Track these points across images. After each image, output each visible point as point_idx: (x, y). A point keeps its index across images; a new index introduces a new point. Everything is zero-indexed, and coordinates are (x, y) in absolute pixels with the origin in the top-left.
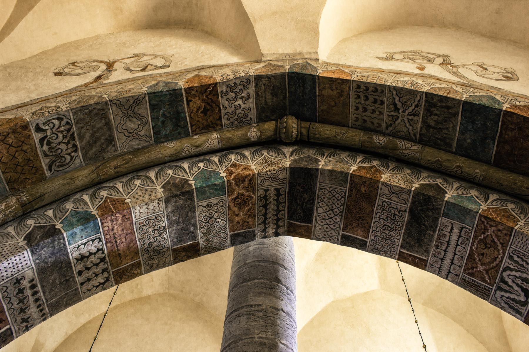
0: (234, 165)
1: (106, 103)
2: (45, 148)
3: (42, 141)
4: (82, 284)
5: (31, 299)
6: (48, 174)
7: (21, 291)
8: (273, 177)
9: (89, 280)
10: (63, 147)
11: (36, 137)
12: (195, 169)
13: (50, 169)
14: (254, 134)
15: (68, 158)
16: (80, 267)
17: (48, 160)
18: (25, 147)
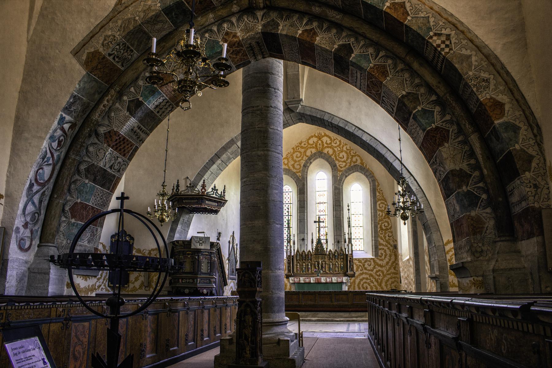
0: (227, 34)
1: (140, 25)
2: (117, 60)
3: (114, 59)
4: (161, 115)
5: (140, 132)
6: (122, 69)
7: (135, 132)
8: (252, 38)
9: (163, 112)
10: (126, 54)
11: (111, 58)
12: (204, 40)
13: (123, 66)
14: (235, 9)
15: (130, 56)
16: (157, 110)
17: (120, 64)
18: (107, 65)
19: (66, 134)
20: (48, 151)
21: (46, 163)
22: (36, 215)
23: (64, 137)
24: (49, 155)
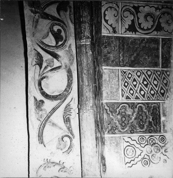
19: (58, 20)
20: (42, 53)
21: (49, 68)
22: (66, 139)
23: (59, 25)
24: (46, 57)
